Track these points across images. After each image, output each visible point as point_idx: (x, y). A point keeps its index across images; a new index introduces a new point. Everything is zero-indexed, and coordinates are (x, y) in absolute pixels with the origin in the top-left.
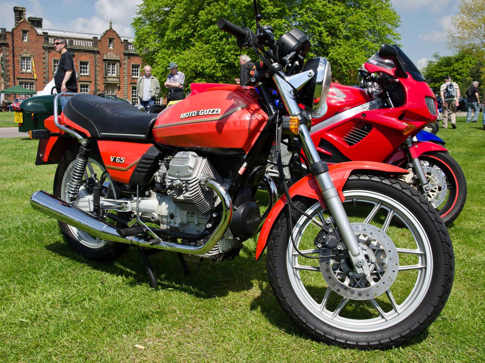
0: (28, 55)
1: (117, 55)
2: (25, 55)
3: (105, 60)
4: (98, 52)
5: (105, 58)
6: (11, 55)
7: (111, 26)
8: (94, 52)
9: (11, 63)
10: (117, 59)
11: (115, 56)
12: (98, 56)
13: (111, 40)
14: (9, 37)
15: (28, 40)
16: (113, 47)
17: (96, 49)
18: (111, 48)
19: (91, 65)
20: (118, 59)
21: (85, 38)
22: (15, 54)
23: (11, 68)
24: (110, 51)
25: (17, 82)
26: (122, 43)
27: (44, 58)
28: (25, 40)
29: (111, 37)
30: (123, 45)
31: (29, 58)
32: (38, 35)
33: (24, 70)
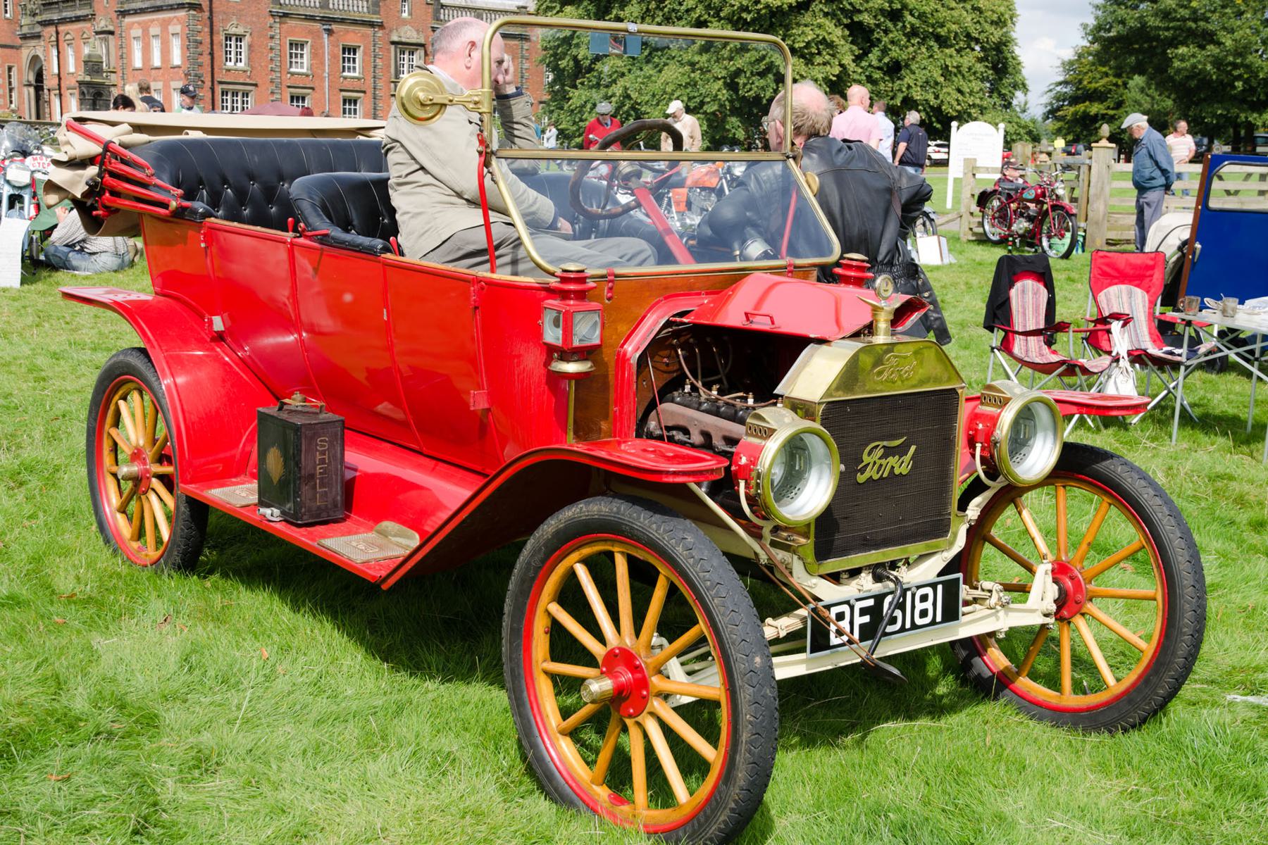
0: (240, 31)
1: (418, 31)
2: (233, 30)
3: (393, 43)
4: (381, 26)
5: (395, 38)
6: (207, 29)
8: (371, 24)
9: (206, 48)
10: (419, 41)
11: (415, 34)
12: (380, 34)
16: (410, 14)
17: (375, 18)
18: (405, 15)
19: (365, 53)
20: (422, 41)
22: (215, 28)
23: (206, 59)
24: (405, 22)
25: (218, 89)
27: (272, 37)
33: (230, 64)
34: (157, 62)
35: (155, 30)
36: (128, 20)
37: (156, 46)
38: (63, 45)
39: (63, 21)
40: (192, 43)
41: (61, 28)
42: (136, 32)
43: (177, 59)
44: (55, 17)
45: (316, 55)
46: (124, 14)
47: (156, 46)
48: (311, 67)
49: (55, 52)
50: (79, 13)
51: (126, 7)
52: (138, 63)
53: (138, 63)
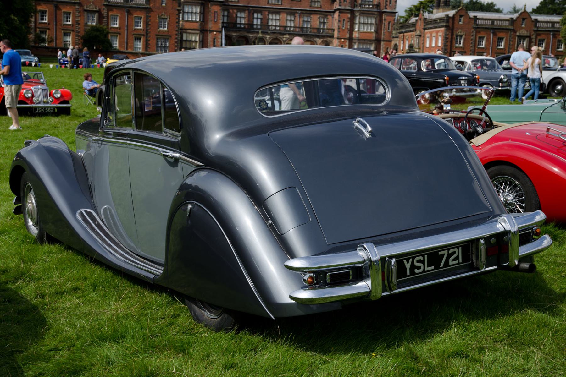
0: (462, 33)
1: (527, 31)
7: (525, 8)
11: (526, 32)
13: (524, 19)
14: (451, 21)
15: (463, 23)
18: (523, 26)
20: (528, 34)
21: (501, 18)
24: (523, 28)
26: (533, 21)
28: (461, 23)
29: (525, 17)
30: (533, 23)
31: (461, 36)
32: (470, 18)
34: (433, 45)
35: (434, 34)
36: (426, 31)
37: (434, 39)
38: (405, 40)
39: (406, 32)
40: (445, 39)
41: (405, 34)
42: (428, 35)
43: (440, 44)
45: (488, 41)
46: (425, 29)
47: (434, 39)
48: (485, 45)
49: (402, 42)
50: (411, 29)
52: (428, 46)
53: (428, 46)
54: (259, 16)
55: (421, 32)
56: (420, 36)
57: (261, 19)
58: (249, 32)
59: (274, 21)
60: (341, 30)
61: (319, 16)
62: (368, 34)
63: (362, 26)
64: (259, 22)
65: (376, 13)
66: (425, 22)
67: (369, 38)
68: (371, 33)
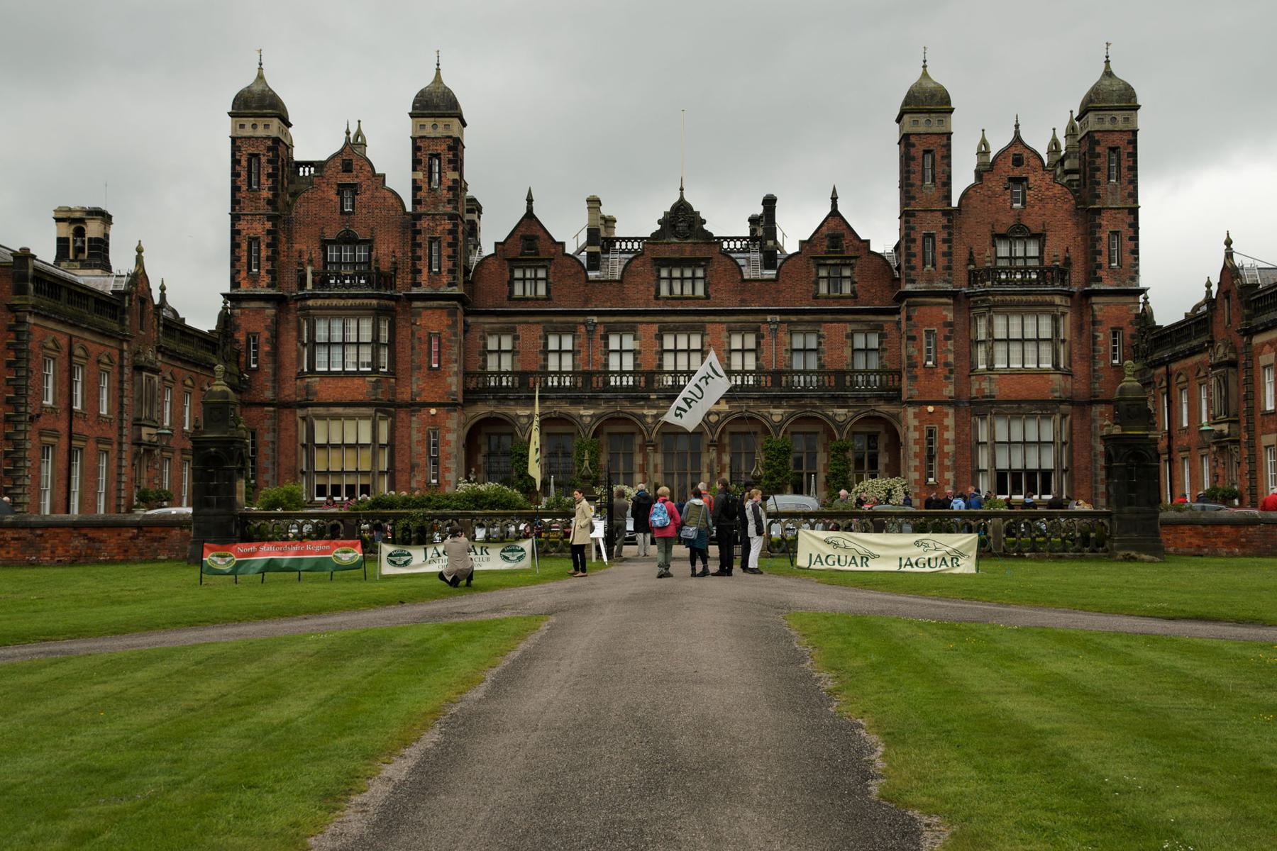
36: (1258, 340)
38: (1175, 390)
39: (1175, 358)
44: (1166, 354)
46: (1250, 332)
51: (1254, 322)
54: (629, 342)
55: (1234, 349)
56: (1233, 364)
57: (635, 352)
58: (576, 401)
59: (682, 359)
60: (919, 371)
61: (849, 328)
62: (1030, 380)
63: (1000, 350)
64: (628, 364)
65: (1057, 300)
66: (1247, 305)
67: (1034, 396)
68: (1040, 373)
